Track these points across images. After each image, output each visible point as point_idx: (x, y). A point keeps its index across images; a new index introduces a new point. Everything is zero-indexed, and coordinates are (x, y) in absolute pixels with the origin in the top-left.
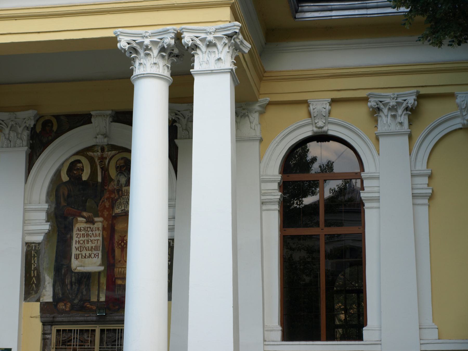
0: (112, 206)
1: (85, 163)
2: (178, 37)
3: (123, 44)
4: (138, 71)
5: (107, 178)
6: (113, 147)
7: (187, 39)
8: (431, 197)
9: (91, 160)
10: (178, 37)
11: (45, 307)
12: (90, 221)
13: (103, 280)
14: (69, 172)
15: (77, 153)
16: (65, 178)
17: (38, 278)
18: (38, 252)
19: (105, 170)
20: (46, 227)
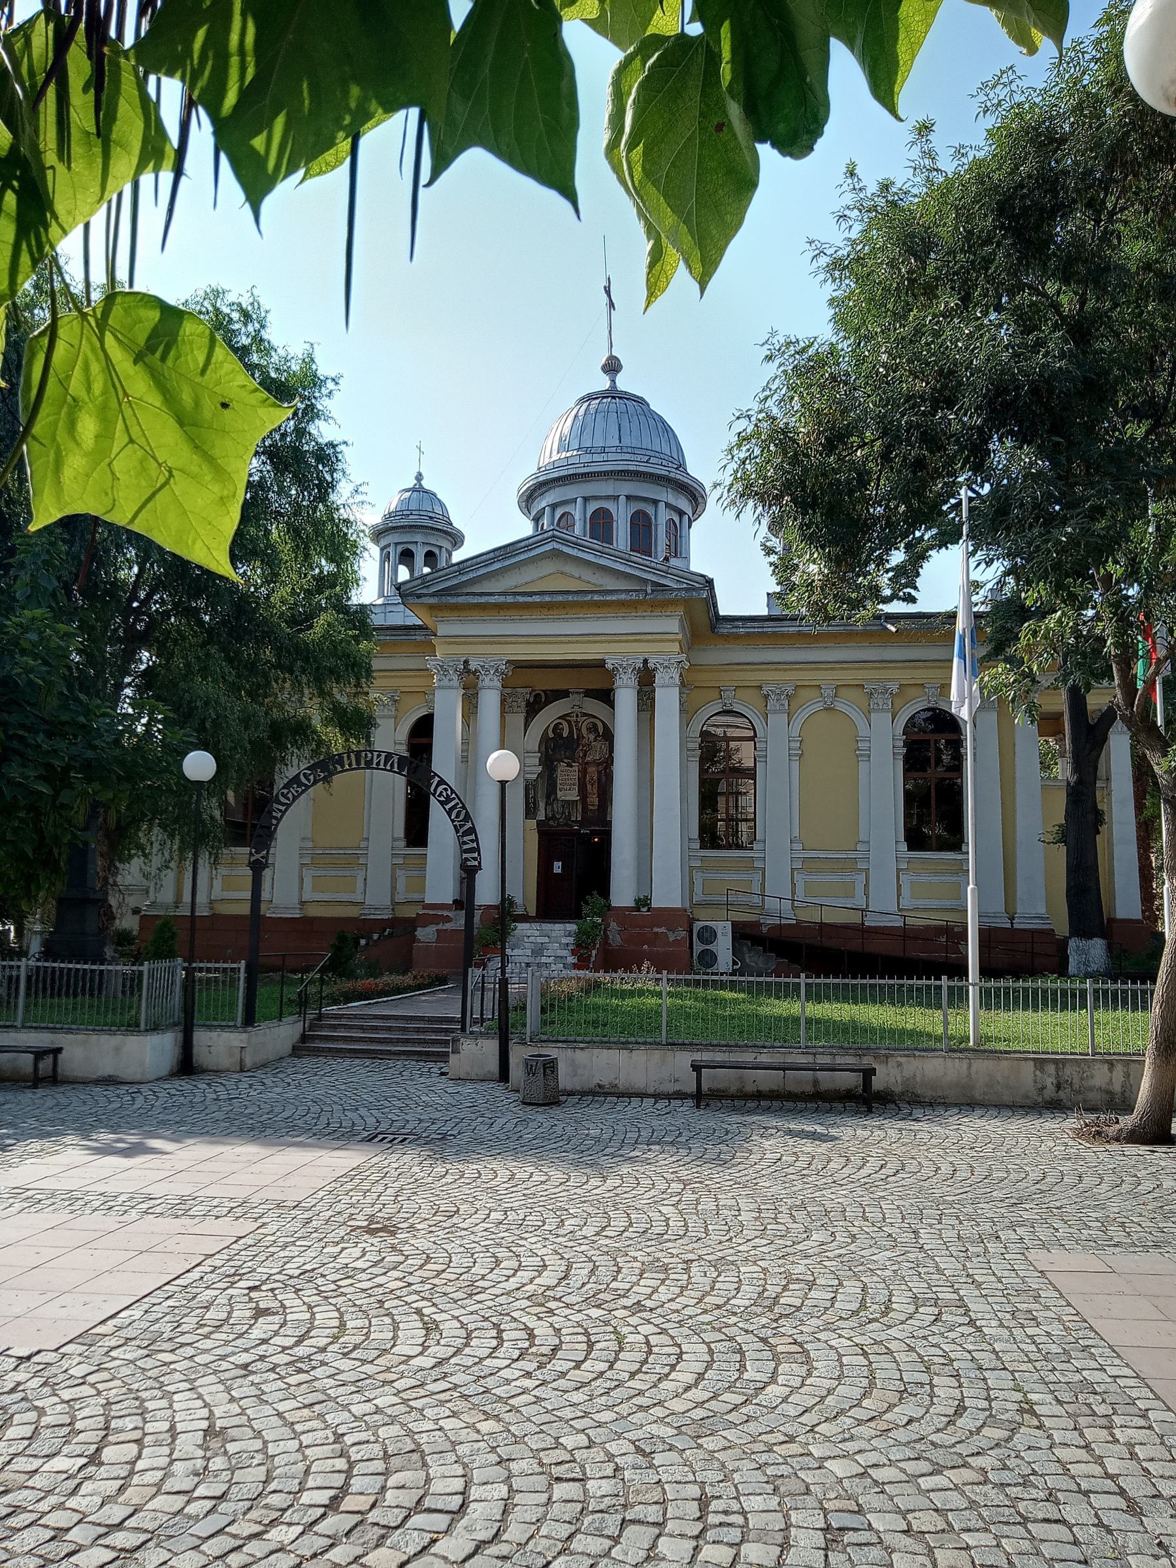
0: (585, 755)
1: (565, 725)
2: (646, 661)
3: (609, 666)
4: (618, 683)
5: (580, 737)
6: (585, 715)
7: (651, 665)
8: (801, 756)
9: (569, 722)
10: (646, 661)
11: (539, 823)
12: (569, 765)
13: (580, 807)
14: (554, 731)
15: (559, 718)
16: (551, 735)
17: (534, 803)
18: (535, 787)
19: (579, 730)
20: (540, 769)
